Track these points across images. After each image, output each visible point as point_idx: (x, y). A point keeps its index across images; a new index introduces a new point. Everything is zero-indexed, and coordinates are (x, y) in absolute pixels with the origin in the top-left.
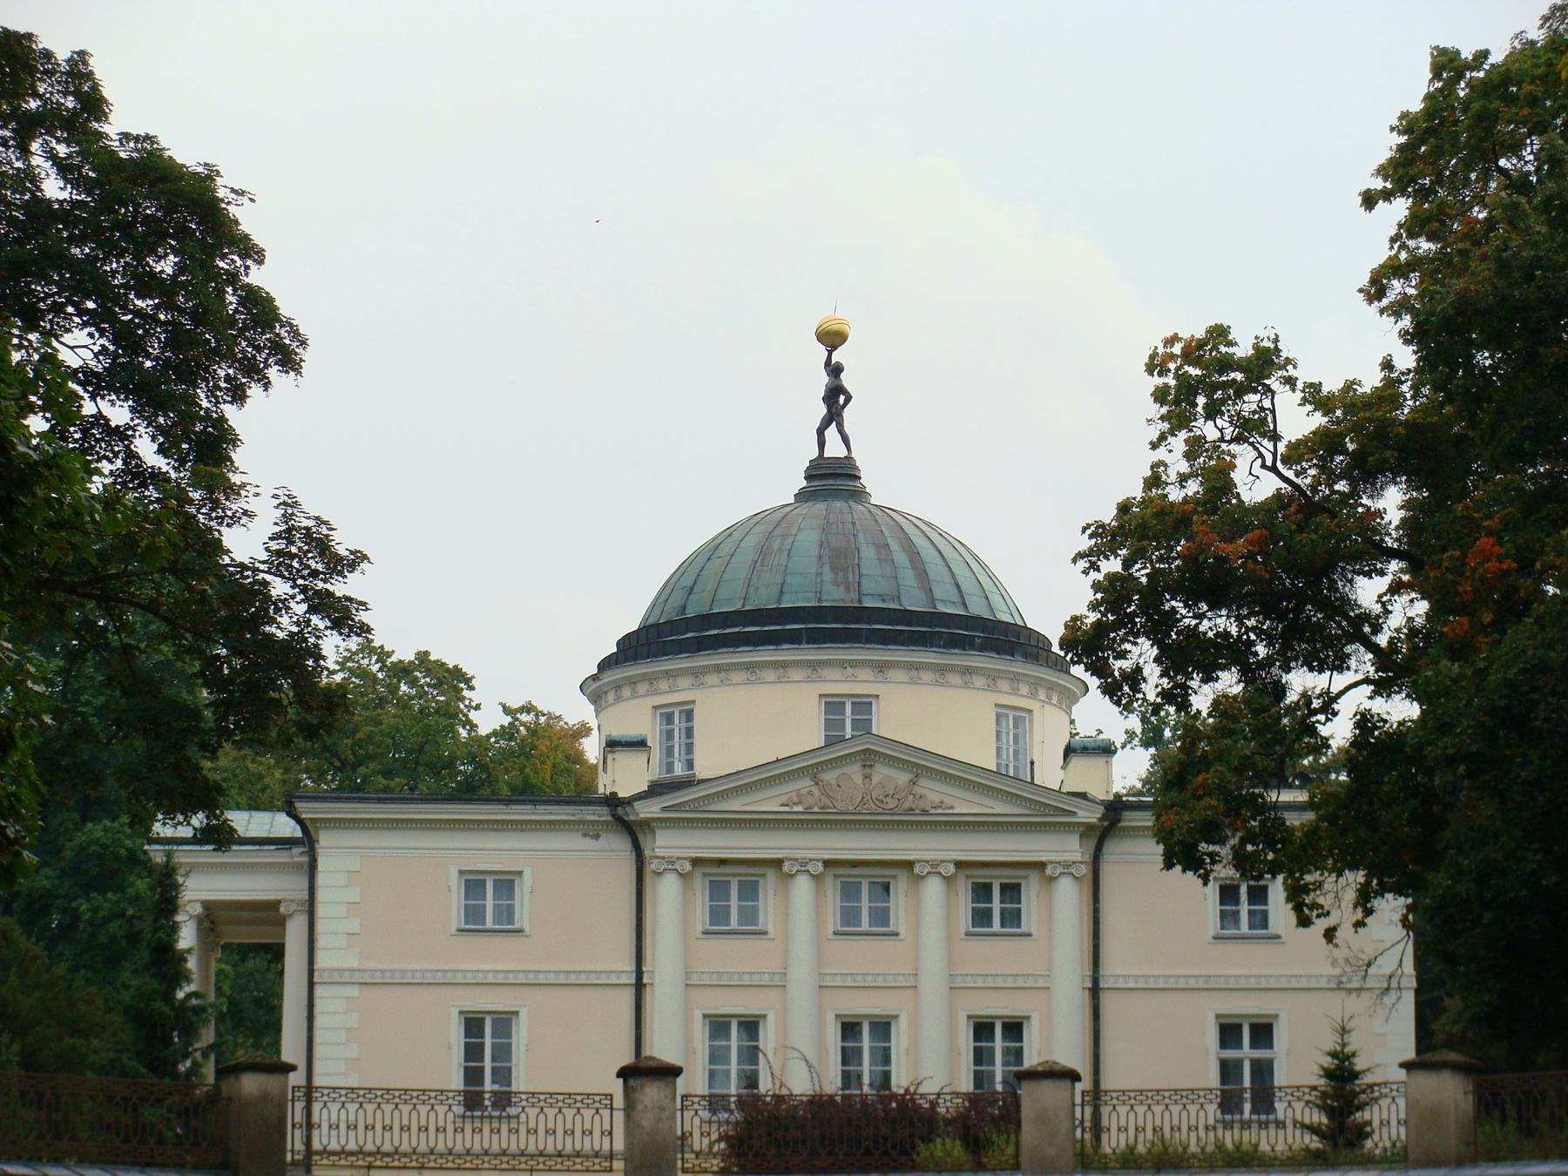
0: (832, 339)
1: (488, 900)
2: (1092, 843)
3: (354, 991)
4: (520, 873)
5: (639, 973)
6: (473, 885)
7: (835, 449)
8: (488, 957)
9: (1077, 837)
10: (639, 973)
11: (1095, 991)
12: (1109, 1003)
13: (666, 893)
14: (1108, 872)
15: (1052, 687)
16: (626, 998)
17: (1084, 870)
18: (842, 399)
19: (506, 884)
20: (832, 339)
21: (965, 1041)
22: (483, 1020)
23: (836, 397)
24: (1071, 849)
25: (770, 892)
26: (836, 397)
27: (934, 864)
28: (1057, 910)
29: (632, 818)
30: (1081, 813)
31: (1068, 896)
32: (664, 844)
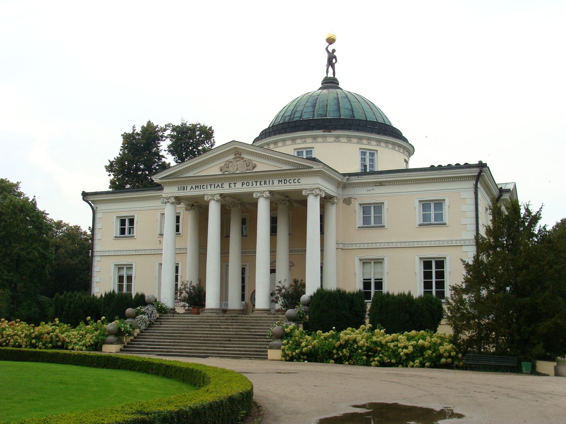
0: (331, 41)
7: (330, 75)
15: (400, 146)
18: (334, 61)
20: (331, 41)
23: (331, 60)
26: (331, 60)
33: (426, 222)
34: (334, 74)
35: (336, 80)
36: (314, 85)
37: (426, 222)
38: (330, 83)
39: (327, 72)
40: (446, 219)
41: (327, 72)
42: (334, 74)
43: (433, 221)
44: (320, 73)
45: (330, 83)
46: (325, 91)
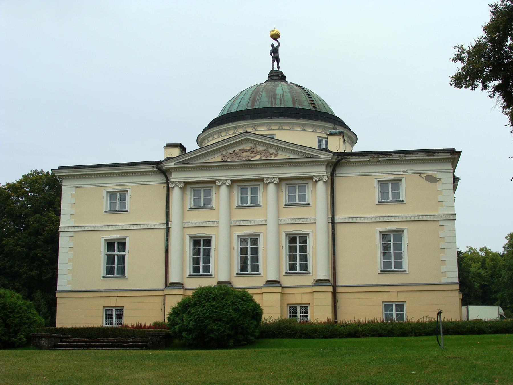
0: (275, 37)
1: (118, 201)
2: (332, 168)
3: (72, 234)
4: (127, 191)
5: (167, 224)
6: (112, 194)
7: (276, 69)
8: (117, 221)
9: (325, 167)
10: (167, 224)
11: (333, 224)
12: (339, 229)
13: (176, 193)
14: (338, 181)
16: (164, 232)
17: (326, 178)
19: (123, 195)
20: (275, 37)
21: (285, 244)
22: (114, 244)
24: (321, 171)
25: (214, 193)
27: (272, 179)
28: (318, 195)
29: (164, 168)
30: (322, 156)
31: (321, 189)
32: (176, 177)
33: (384, 201)
34: (278, 68)
35: (282, 73)
36: (260, 76)
37: (384, 201)
38: (277, 76)
39: (273, 66)
40: (403, 196)
41: (273, 66)
42: (278, 68)
43: (391, 199)
44: (267, 66)
45: (277, 76)
46: (269, 83)
